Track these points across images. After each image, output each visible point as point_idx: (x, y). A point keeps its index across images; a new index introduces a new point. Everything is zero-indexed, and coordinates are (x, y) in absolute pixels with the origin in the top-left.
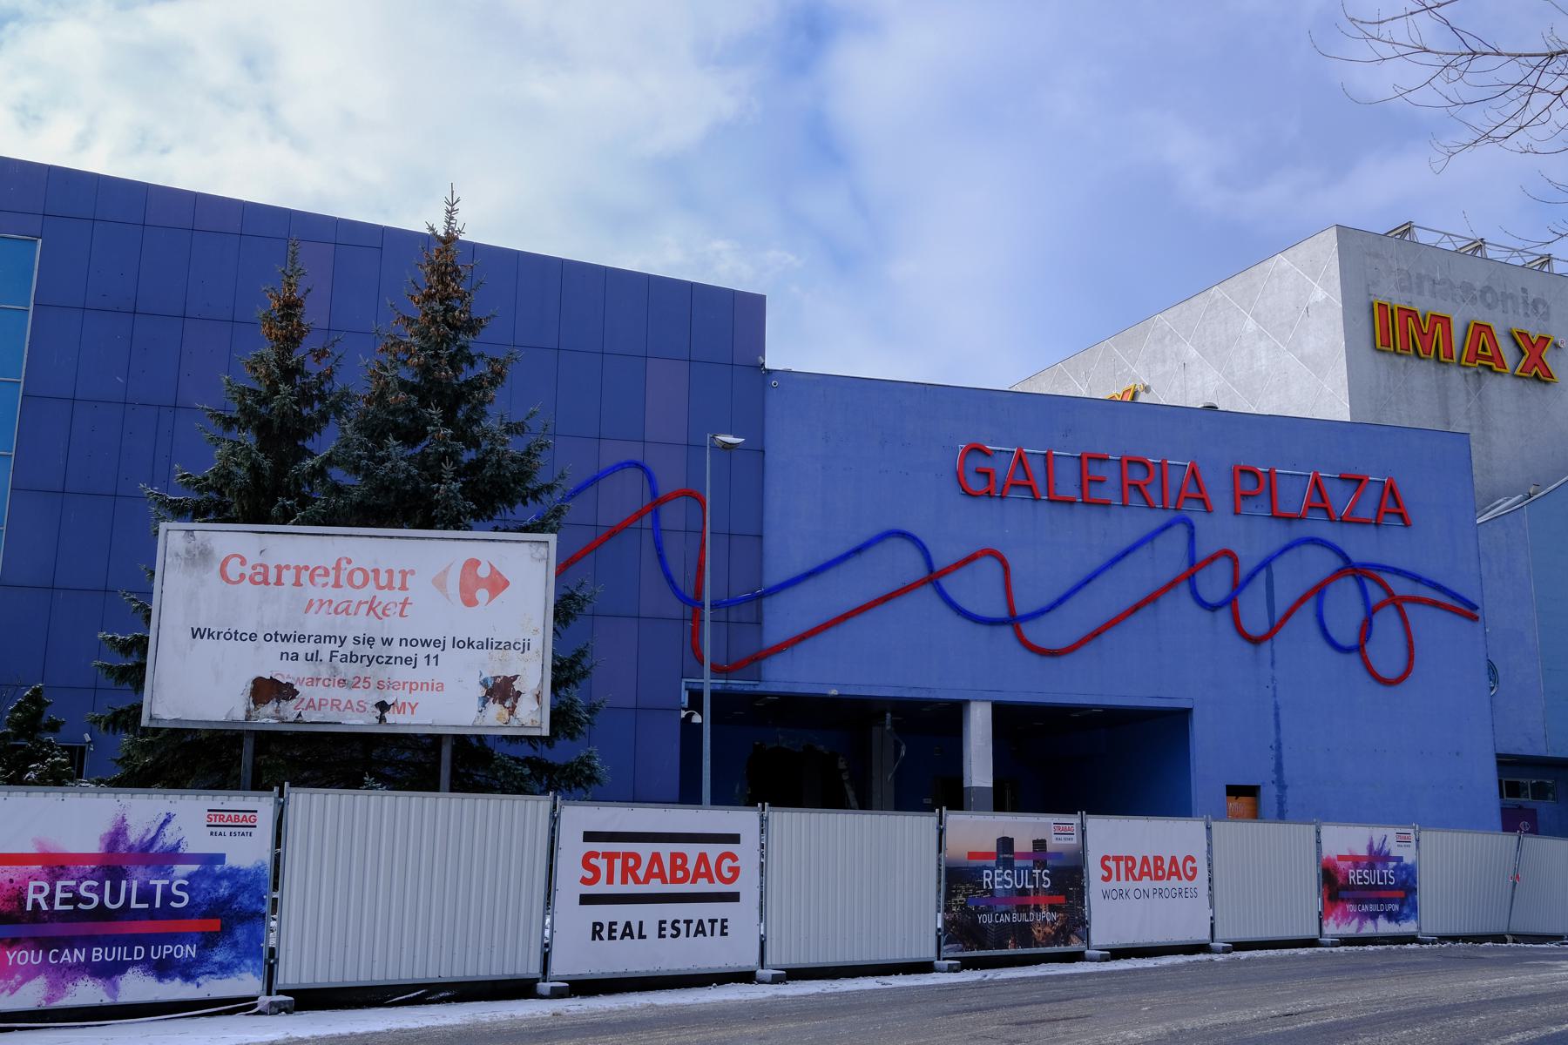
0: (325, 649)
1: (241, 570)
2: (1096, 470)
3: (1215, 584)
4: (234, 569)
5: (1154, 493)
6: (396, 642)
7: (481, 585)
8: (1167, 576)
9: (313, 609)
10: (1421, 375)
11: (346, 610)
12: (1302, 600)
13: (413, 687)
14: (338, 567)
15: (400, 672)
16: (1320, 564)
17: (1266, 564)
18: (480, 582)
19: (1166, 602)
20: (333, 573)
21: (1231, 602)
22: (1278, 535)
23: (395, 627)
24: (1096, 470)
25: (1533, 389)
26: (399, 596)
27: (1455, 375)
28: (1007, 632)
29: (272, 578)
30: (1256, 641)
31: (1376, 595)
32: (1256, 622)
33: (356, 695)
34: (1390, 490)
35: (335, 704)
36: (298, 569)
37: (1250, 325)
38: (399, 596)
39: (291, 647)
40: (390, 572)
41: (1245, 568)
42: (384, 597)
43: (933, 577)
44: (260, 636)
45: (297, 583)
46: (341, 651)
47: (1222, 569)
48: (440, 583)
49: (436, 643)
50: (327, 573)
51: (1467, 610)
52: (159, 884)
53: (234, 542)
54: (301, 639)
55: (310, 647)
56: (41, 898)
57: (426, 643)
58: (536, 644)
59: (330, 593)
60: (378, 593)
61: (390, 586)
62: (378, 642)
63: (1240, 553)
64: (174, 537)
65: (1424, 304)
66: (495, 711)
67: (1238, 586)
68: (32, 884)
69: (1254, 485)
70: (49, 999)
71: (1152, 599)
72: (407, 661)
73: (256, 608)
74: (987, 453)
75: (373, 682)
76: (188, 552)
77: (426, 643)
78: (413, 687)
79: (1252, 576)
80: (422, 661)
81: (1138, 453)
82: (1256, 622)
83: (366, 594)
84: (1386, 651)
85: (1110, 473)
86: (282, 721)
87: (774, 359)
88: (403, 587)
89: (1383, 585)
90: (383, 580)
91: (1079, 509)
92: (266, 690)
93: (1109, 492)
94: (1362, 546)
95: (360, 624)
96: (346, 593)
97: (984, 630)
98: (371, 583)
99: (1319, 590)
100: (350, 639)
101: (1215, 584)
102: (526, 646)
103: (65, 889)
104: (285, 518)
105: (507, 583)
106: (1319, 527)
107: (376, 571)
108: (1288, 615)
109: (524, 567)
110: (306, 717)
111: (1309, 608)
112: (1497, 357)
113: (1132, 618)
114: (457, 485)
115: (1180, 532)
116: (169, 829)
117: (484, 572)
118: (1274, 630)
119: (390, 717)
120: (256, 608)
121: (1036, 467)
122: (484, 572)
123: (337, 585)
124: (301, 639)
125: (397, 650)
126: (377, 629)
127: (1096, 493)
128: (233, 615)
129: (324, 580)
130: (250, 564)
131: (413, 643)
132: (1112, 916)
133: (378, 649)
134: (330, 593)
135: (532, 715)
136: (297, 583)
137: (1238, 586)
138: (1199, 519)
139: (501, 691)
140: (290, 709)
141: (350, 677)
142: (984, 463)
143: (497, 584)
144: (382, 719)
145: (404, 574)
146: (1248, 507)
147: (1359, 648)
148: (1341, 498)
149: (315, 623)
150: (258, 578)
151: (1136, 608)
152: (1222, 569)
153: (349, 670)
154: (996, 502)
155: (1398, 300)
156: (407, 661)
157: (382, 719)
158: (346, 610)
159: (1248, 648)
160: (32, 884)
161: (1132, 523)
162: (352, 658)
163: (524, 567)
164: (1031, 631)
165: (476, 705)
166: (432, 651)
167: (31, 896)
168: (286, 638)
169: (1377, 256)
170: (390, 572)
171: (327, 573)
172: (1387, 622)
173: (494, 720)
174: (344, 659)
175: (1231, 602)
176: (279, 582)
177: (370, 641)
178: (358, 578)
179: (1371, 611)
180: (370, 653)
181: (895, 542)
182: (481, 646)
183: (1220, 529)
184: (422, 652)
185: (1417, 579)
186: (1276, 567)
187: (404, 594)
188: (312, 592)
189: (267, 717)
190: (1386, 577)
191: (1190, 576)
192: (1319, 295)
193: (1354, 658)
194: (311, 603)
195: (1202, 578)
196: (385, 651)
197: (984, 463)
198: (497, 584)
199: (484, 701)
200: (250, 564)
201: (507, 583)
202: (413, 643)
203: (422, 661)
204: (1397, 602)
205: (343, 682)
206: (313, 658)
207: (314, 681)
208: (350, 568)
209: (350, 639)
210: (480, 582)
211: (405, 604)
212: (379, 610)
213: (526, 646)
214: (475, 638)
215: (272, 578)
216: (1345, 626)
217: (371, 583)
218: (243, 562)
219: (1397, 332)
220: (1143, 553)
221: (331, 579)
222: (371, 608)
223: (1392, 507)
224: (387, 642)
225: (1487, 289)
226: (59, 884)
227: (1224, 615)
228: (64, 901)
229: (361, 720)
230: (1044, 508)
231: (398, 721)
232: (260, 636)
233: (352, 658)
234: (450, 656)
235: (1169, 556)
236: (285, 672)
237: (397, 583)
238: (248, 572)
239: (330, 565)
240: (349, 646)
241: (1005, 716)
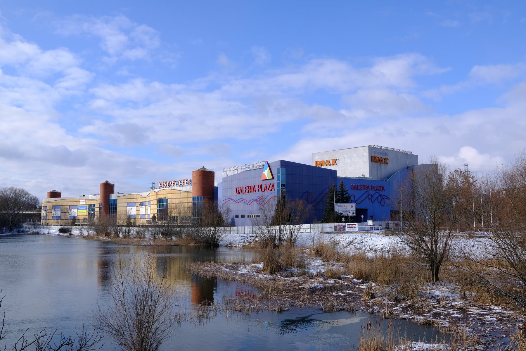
3: (370, 197)
7: (352, 207)
34: (383, 187)
37: (355, 155)
51: (388, 199)
53: (339, 204)
94: (381, 193)
99: (377, 197)
101: (370, 197)
106: (378, 191)
132: (347, 230)
139: (353, 213)
147: (380, 203)
148: (379, 188)
161: (364, 191)
172: (383, 200)
180: (346, 211)
183: (371, 192)
191: (368, 196)
192: (365, 154)
204: (383, 198)
216: (379, 201)
223: (383, 189)
235: (366, 195)
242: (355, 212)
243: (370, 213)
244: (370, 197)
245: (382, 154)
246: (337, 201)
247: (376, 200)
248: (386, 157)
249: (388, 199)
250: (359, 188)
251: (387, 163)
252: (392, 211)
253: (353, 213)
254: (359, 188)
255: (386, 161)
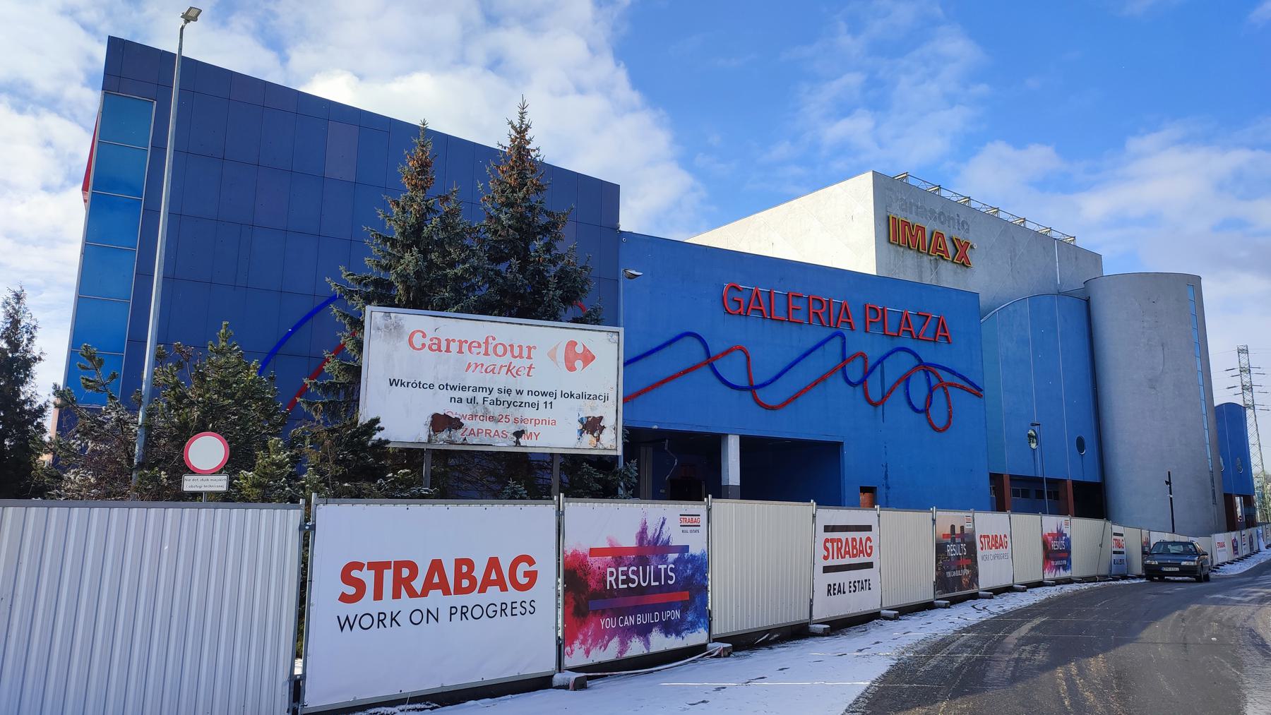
0: (480, 396)
1: (423, 341)
2: (795, 303)
3: (855, 372)
4: (418, 340)
5: (824, 318)
6: (525, 393)
7: (577, 358)
8: (831, 366)
9: (472, 368)
10: (910, 257)
11: (493, 371)
12: (898, 382)
13: (536, 422)
14: (486, 342)
15: (528, 413)
16: (904, 362)
17: (880, 361)
18: (577, 356)
19: (830, 380)
20: (483, 346)
21: (863, 381)
22: (885, 345)
23: (525, 383)
24: (795, 303)
25: (960, 270)
26: (527, 363)
27: (926, 259)
28: (748, 394)
29: (444, 348)
30: (875, 405)
31: (934, 381)
32: (876, 395)
33: (501, 427)
34: (941, 325)
35: (488, 432)
36: (460, 341)
38: (527, 363)
39: (457, 394)
40: (521, 347)
41: (871, 363)
42: (517, 363)
43: (710, 361)
44: (436, 386)
45: (460, 352)
46: (491, 397)
47: (859, 362)
48: (552, 355)
49: (550, 394)
50: (479, 346)
52: (663, 567)
53: (415, 321)
54: (463, 388)
55: (470, 394)
56: (613, 579)
57: (544, 394)
58: (613, 397)
59: (482, 359)
60: (513, 360)
61: (521, 356)
62: (514, 392)
63: (868, 354)
64: (375, 315)
65: (912, 219)
66: (588, 439)
67: (867, 373)
68: (609, 570)
69: (875, 315)
70: (621, 652)
71: (823, 378)
72: (532, 405)
73: (433, 367)
74: (738, 289)
75: (512, 419)
76: (386, 327)
77: (544, 394)
78: (536, 422)
79: (874, 367)
80: (542, 406)
81: (817, 295)
82: (876, 395)
83: (508, 358)
84: (938, 413)
85: (801, 304)
86: (452, 443)
87: (625, 224)
88: (529, 357)
89: (938, 377)
90: (516, 352)
91: (786, 324)
92: (441, 422)
93: (801, 316)
94: (929, 353)
95: (502, 380)
96: (492, 359)
97: (736, 393)
98: (509, 354)
99: (906, 379)
100: (495, 390)
102: (606, 398)
103: (624, 573)
104: (443, 306)
105: (594, 358)
106: (907, 342)
107: (512, 346)
108: (890, 392)
109: (604, 346)
110: (469, 441)
111: (901, 387)
112: (945, 251)
113: (815, 389)
114: (559, 292)
115: (837, 341)
116: (664, 529)
117: (579, 349)
118: (884, 398)
119: (522, 441)
120: (433, 367)
121: (764, 299)
122: (579, 349)
123: (486, 354)
124: (463, 388)
125: (526, 398)
126: (513, 384)
127: (794, 316)
128: (414, 369)
129: (478, 350)
130: (429, 336)
131: (536, 393)
133: (513, 397)
134: (482, 359)
135: (610, 442)
136: (460, 352)
137: (867, 373)
138: (847, 332)
139: (592, 426)
140: (458, 435)
141: (496, 415)
142: (736, 295)
143: (588, 358)
144: (518, 443)
145: (529, 348)
146: (872, 329)
147: (926, 411)
149: (472, 379)
150: (435, 347)
151: (815, 384)
152: (859, 362)
153: (495, 411)
154: (743, 318)
155: (901, 216)
156: (532, 405)
157: (518, 443)
158: (493, 371)
159: (872, 408)
160: (609, 570)
161: (815, 334)
162: (497, 402)
163: (604, 346)
164: (760, 393)
165: (576, 434)
166: (548, 399)
167: (609, 579)
168: (453, 388)
169: (891, 190)
170: (521, 347)
171: (479, 346)
172: (939, 396)
173: (587, 445)
174: (492, 403)
175: (863, 381)
176: (448, 350)
177: (509, 392)
178: (500, 350)
179: (931, 390)
180: (509, 399)
181: (687, 339)
182: (579, 397)
184: (542, 399)
185: (953, 372)
186: (885, 362)
187: (530, 362)
188: (470, 358)
189: (442, 440)
190: (938, 371)
191: (842, 368)
193: (923, 416)
194: (469, 366)
195: (849, 367)
196: (519, 398)
197: (736, 295)
198: (588, 358)
199: (581, 432)
200: (429, 336)
201: (594, 358)
202: (536, 393)
203: (542, 406)
204: (944, 386)
205: (492, 419)
206: (472, 401)
207: (473, 416)
208: (494, 343)
209: (495, 390)
210: (577, 356)
211: (530, 368)
212: (514, 371)
213: (606, 398)
214: (575, 392)
215: (444, 348)
216: (919, 399)
217: (509, 354)
218: (424, 336)
219: (896, 232)
220: (819, 352)
221: (482, 350)
222: (509, 370)
223: (941, 332)
224: (520, 392)
225: (941, 213)
226: (620, 569)
227: (859, 389)
228: (623, 582)
229: (504, 444)
230: (768, 322)
231: (529, 444)
232: (436, 386)
233: (497, 402)
234: (560, 403)
236: (455, 411)
237: (525, 354)
238: (428, 342)
239: (482, 341)
240: (495, 395)
241: (747, 444)
242: (610, 413)
243: (854, 465)
244: (860, 376)
245: (941, 217)
246: (383, 295)
247: (899, 393)
248: (961, 235)
249: (977, 391)
250: (780, 312)
251: (965, 264)
252: (996, 478)
253: (592, 426)
254: (780, 312)
255: (961, 255)
